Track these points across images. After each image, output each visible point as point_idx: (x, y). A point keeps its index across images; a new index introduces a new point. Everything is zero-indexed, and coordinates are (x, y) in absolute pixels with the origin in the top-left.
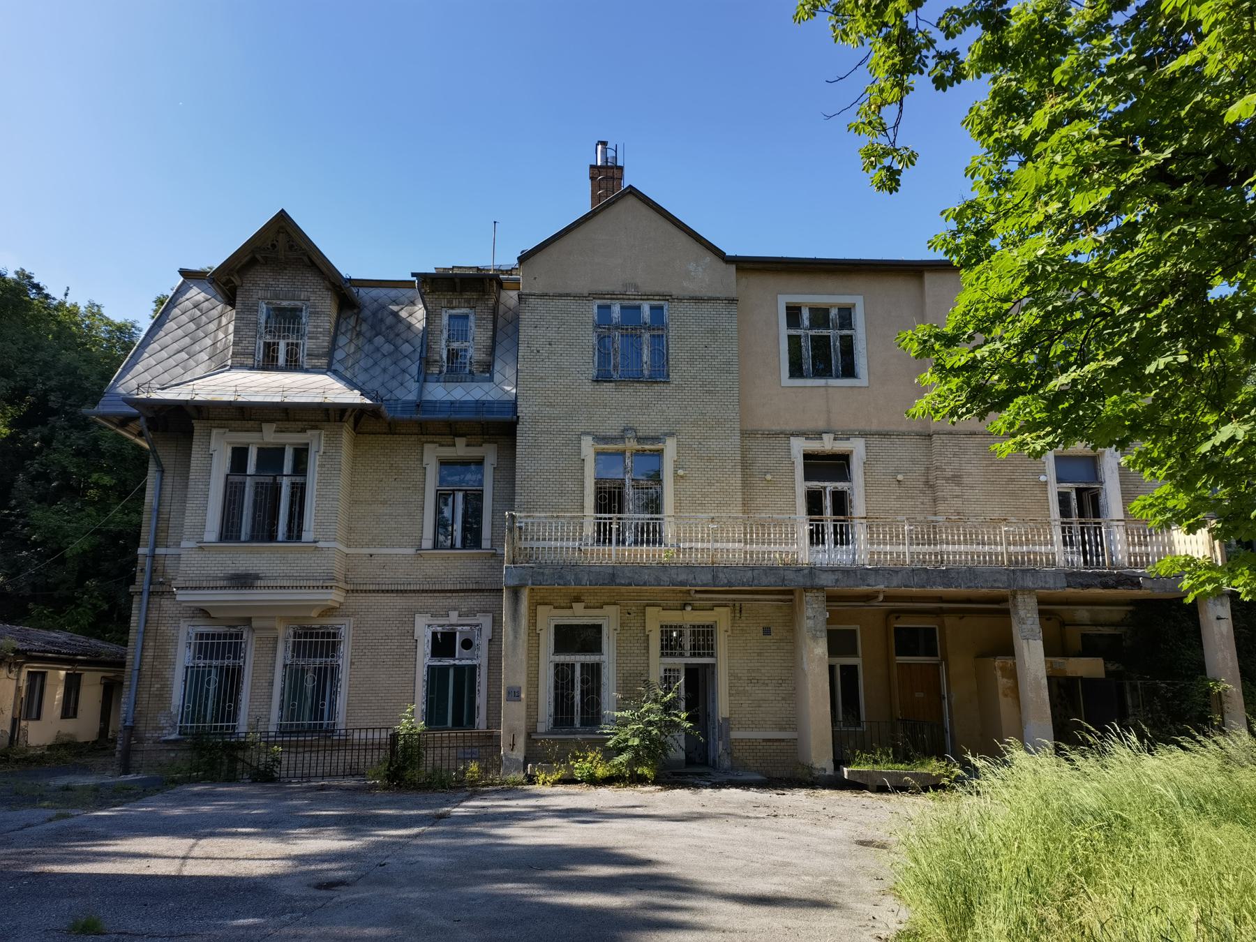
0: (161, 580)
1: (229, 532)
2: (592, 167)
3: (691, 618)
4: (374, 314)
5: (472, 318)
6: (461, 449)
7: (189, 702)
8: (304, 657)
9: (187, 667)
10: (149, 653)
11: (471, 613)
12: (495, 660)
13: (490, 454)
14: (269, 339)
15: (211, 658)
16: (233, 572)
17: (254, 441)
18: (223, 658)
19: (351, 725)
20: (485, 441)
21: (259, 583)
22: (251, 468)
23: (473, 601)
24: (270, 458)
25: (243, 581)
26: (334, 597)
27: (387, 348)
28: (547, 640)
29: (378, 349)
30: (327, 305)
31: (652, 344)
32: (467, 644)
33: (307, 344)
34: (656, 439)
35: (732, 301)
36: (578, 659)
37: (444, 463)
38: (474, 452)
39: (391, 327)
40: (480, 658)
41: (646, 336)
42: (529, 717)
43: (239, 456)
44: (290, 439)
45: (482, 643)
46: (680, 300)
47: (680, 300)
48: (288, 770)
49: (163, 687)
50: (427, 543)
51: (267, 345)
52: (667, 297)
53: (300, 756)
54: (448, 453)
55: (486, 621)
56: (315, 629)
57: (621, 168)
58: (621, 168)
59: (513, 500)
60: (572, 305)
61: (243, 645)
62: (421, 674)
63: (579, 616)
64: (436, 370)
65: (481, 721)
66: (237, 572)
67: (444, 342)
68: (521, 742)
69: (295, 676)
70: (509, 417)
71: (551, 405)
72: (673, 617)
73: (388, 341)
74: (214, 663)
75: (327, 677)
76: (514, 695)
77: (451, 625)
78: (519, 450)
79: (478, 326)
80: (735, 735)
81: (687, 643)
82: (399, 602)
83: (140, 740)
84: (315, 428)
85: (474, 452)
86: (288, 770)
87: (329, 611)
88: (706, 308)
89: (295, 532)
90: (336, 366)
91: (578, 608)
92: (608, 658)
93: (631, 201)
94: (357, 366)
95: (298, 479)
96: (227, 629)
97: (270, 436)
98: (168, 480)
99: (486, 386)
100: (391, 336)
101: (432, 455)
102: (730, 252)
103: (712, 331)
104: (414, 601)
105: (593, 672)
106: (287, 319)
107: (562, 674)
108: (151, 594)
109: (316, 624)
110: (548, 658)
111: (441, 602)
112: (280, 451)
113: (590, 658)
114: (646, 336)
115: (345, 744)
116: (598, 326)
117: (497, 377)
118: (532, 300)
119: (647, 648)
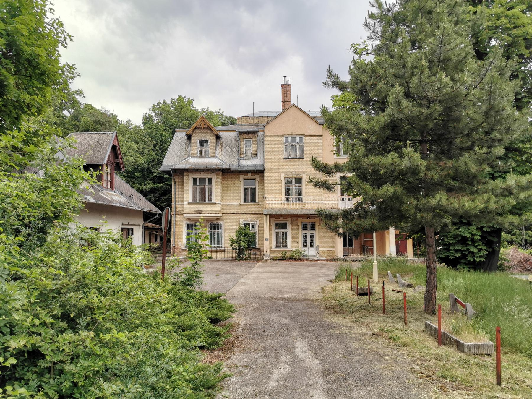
1: (194, 199)
2: (282, 85)
3: (308, 221)
4: (225, 140)
5: (251, 141)
6: (249, 176)
10: (177, 228)
11: (254, 219)
12: (262, 231)
13: (257, 177)
14: (200, 149)
17: (198, 176)
19: (225, 247)
20: (256, 174)
21: (203, 212)
22: (198, 184)
23: (254, 216)
24: (203, 180)
25: (199, 212)
26: (219, 215)
27: (230, 150)
28: (274, 226)
29: (227, 150)
30: (214, 139)
31: (300, 148)
32: (253, 227)
33: (209, 150)
34: (301, 174)
35: (321, 136)
36: (282, 231)
37: (245, 179)
38: (253, 177)
39: (230, 144)
40: (256, 230)
41: (298, 146)
42: (270, 245)
43: (195, 180)
44: (207, 176)
45: (256, 226)
46: (307, 136)
47: (307, 136)
49: (180, 237)
50: (242, 201)
51: (200, 151)
52: (303, 135)
54: (246, 177)
55: (258, 221)
57: (291, 85)
58: (291, 85)
59: (264, 190)
60: (278, 138)
63: (281, 220)
64: (242, 156)
65: (257, 246)
67: (244, 149)
68: (269, 251)
70: (262, 169)
71: (273, 166)
72: (305, 221)
73: (230, 148)
75: (219, 235)
76: (267, 240)
78: (265, 178)
79: (253, 144)
80: (320, 249)
81: (308, 227)
82: (236, 216)
84: (214, 173)
85: (253, 177)
87: (218, 219)
88: (314, 137)
89: (210, 199)
90: (217, 156)
91: (281, 218)
92: (289, 231)
93: (293, 109)
94: (222, 156)
95: (210, 186)
97: (202, 175)
98: (177, 186)
99: (256, 160)
100: (230, 146)
101: (242, 178)
103: (316, 144)
105: (285, 234)
106: (203, 142)
107: (278, 234)
108: (176, 214)
109: (215, 222)
110: (274, 231)
111: (246, 216)
112: (205, 179)
113: (284, 231)
114: (298, 146)
115: (224, 251)
116: (285, 143)
117: (258, 157)
118: (268, 138)
119: (298, 228)
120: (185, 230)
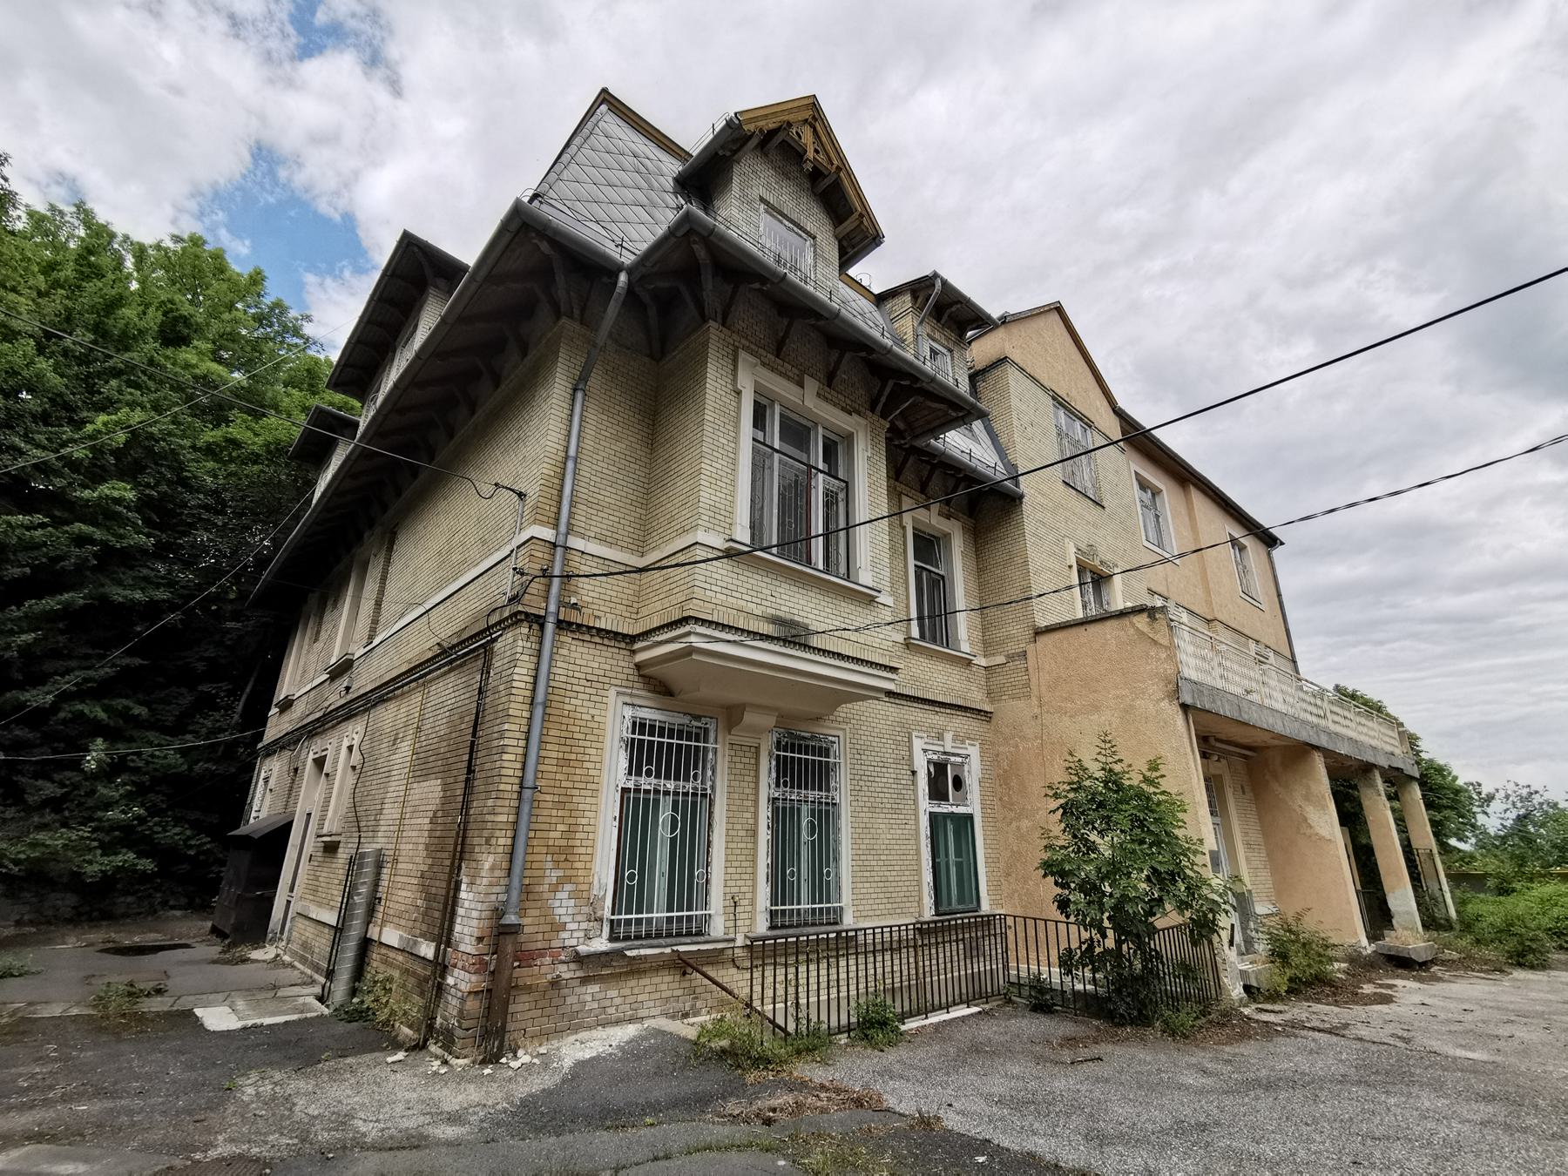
0: (573, 600)
7: (632, 866)
8: (799, 787)
9: (625, 791)
10: (552, 752)
15: (668, 777)
16: (773, 612)
18: (687, 779)
25: (793, 635)
48: (774, 1003)
49: (571, 832)
53: (781, 971)
56: (804, 738)
61: (710, 755)
62: (924, 822)
66: (778, 613)
69: (783, 817)
74: (671, 785)
77: (945, 753)
83: (526, 958)
86: (774, 1003)
96: (686, 720)
102: (1122, 403)
104: (914, 714)
115: (846, 944)
120: (614, 769)
